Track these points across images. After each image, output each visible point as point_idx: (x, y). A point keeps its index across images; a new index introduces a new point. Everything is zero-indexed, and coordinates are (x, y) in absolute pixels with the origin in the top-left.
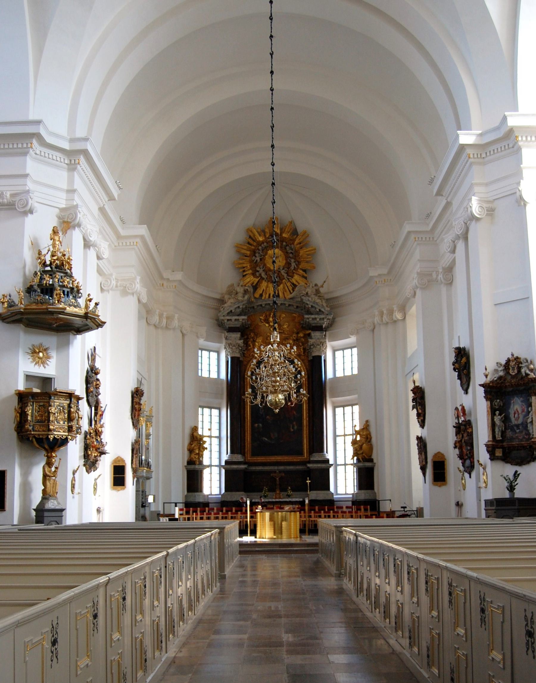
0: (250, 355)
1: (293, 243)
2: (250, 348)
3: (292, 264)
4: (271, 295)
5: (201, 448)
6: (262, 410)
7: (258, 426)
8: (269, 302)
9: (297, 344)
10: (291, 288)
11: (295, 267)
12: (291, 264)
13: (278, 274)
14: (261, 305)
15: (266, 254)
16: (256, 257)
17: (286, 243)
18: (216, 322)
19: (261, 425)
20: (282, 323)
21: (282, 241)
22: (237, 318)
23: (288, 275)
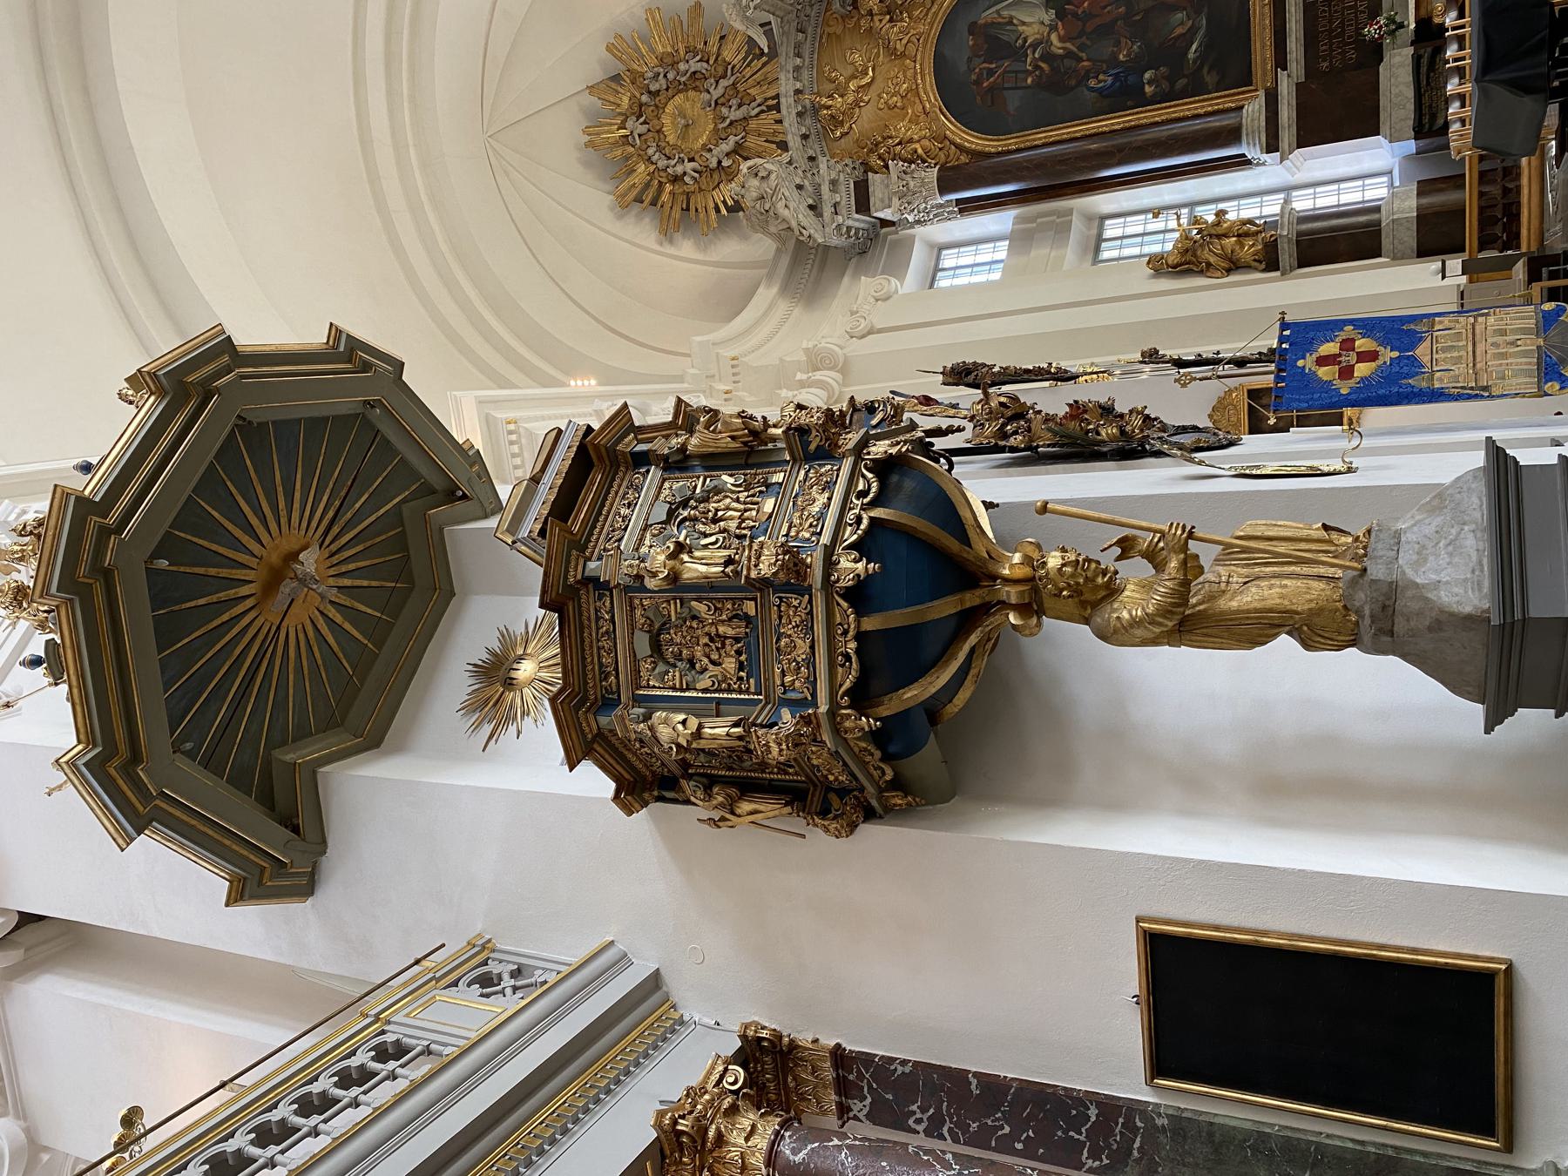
0: (940, 149)
1: (642, 75)
2: (920, 151)
3: (692, 70)
4: (777, 116)
5: (1219, 230)
6: (1100, 82)
7: (1150, 83)
8: (794, 112)
9: (901, 13)
10: (757, 64)
11: (700, 60)
12: (695, 73)
13: (723, 104)
14: (805, 137)
15: (674, 147)
16: (685, 174)
17: (642, 94)
18: (854, 261)
19: (1147, 75)
20: (849, 71)
21: (641, 105)
22: (825, 189)
23: (724, 76)
